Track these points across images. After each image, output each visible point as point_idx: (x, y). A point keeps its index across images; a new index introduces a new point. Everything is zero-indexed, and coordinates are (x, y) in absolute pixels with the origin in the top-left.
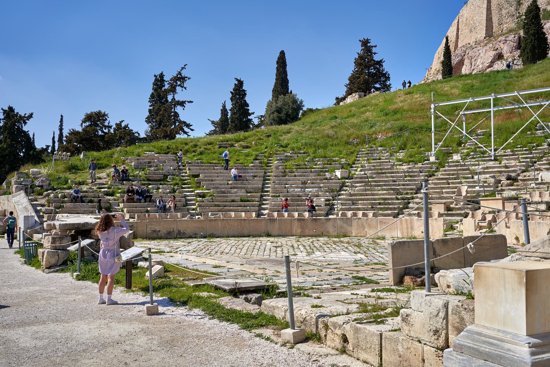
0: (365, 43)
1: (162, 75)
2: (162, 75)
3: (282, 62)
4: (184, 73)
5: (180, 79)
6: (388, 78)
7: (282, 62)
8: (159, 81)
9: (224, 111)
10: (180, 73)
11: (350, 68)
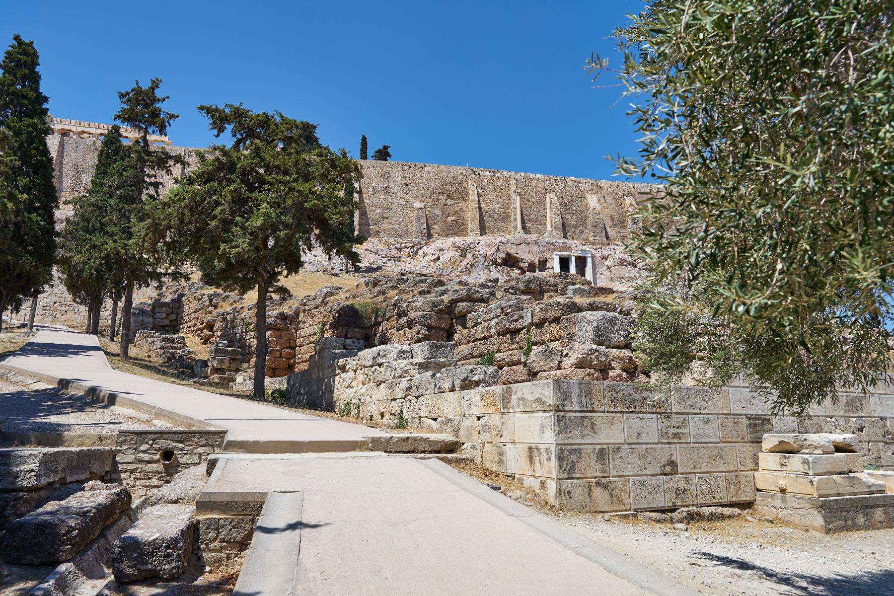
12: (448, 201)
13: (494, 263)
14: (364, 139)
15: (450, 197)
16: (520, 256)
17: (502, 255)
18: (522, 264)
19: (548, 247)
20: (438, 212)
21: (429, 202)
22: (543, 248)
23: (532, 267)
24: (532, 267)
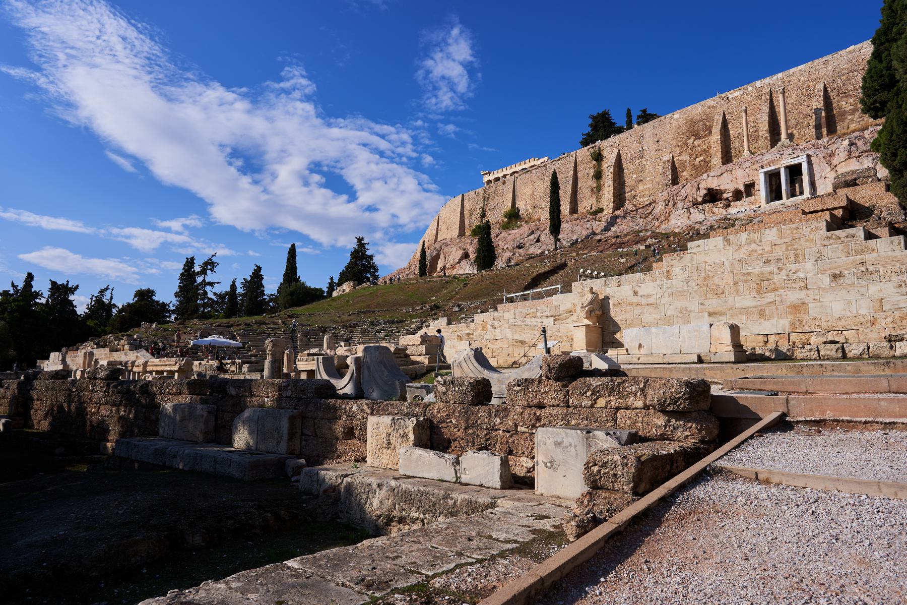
0: (360, 240)
1: (193, 259)
2: (193, 259)
3: (292, 252)
4: (214, 260)
5: (210, 264)
6: (377, 270)
7: (292, 252)
8: (190, 263)
9: (233, 287)
10: (210, 259)
11: (347, 259)
12: (696, 143)
13: (695, 204)
14: (629, 110)
15: (698, 137)
16: (722, 188)
17: (703, 192)
18: (725, 196)
19: (754, 167)
20: (685, 157)
21: (677, 151)
22: (747, 170)
23: (738, 195)
24: (738, 195)
